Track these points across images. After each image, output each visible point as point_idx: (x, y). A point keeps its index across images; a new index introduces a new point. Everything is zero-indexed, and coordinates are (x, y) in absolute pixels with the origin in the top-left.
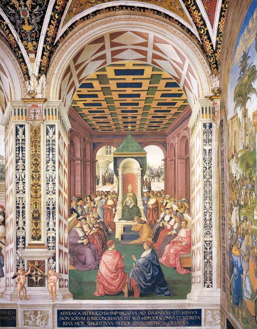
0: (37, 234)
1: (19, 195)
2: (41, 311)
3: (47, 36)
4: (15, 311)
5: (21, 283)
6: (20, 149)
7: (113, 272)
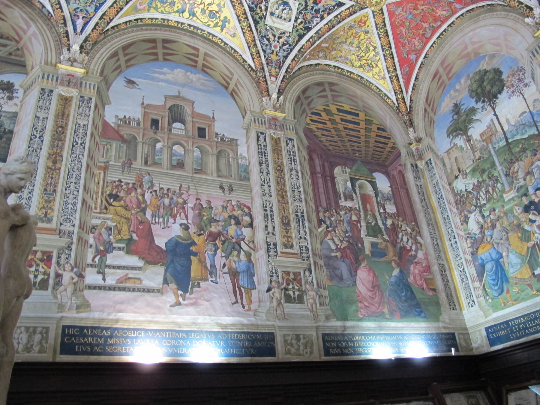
0: (288, 242)
1: (265, 198)
2: (304, 335)
3: (288, 68)
4: (272, 334)
5: (277, 299)
6: (262, 154)
7: (370, 291)
